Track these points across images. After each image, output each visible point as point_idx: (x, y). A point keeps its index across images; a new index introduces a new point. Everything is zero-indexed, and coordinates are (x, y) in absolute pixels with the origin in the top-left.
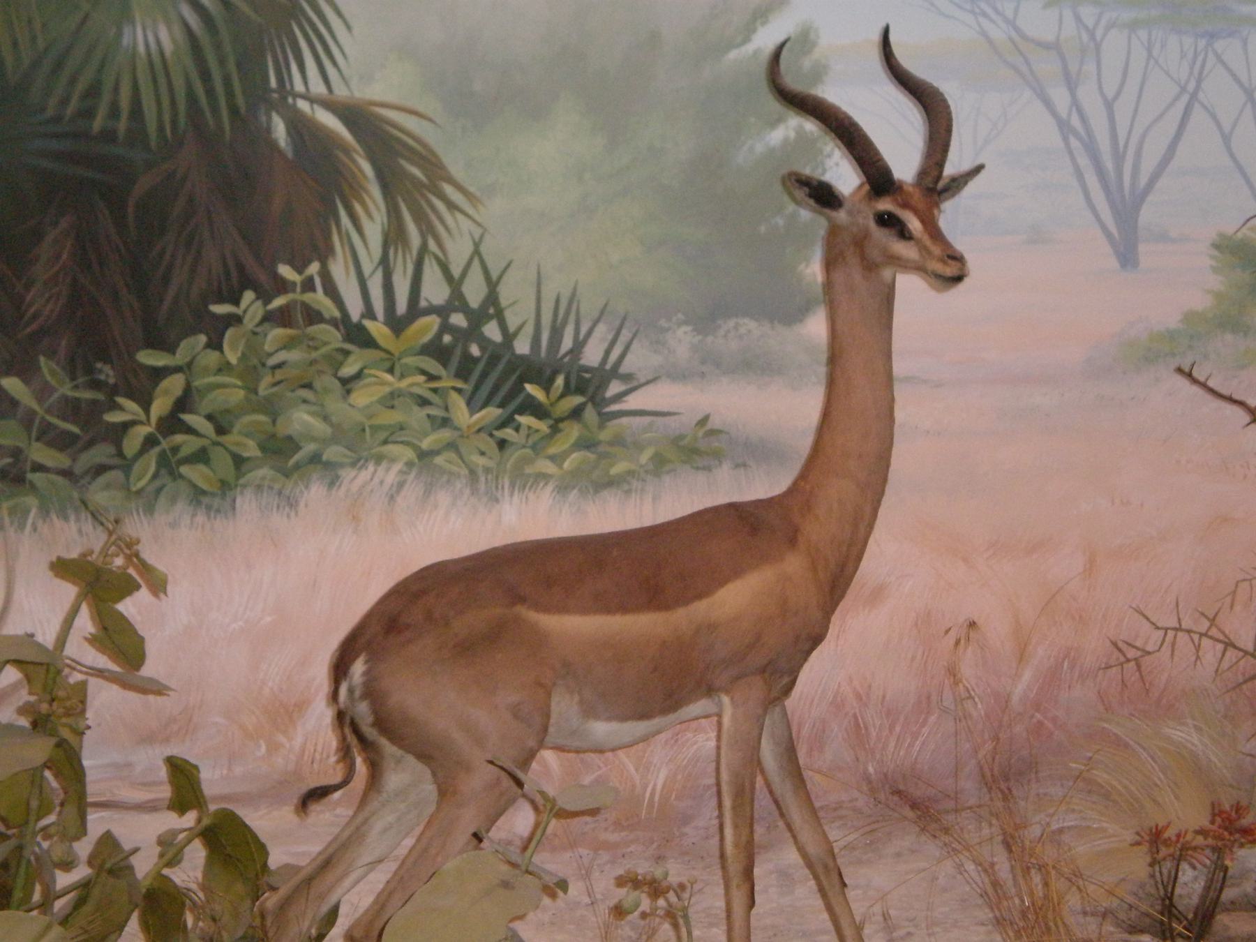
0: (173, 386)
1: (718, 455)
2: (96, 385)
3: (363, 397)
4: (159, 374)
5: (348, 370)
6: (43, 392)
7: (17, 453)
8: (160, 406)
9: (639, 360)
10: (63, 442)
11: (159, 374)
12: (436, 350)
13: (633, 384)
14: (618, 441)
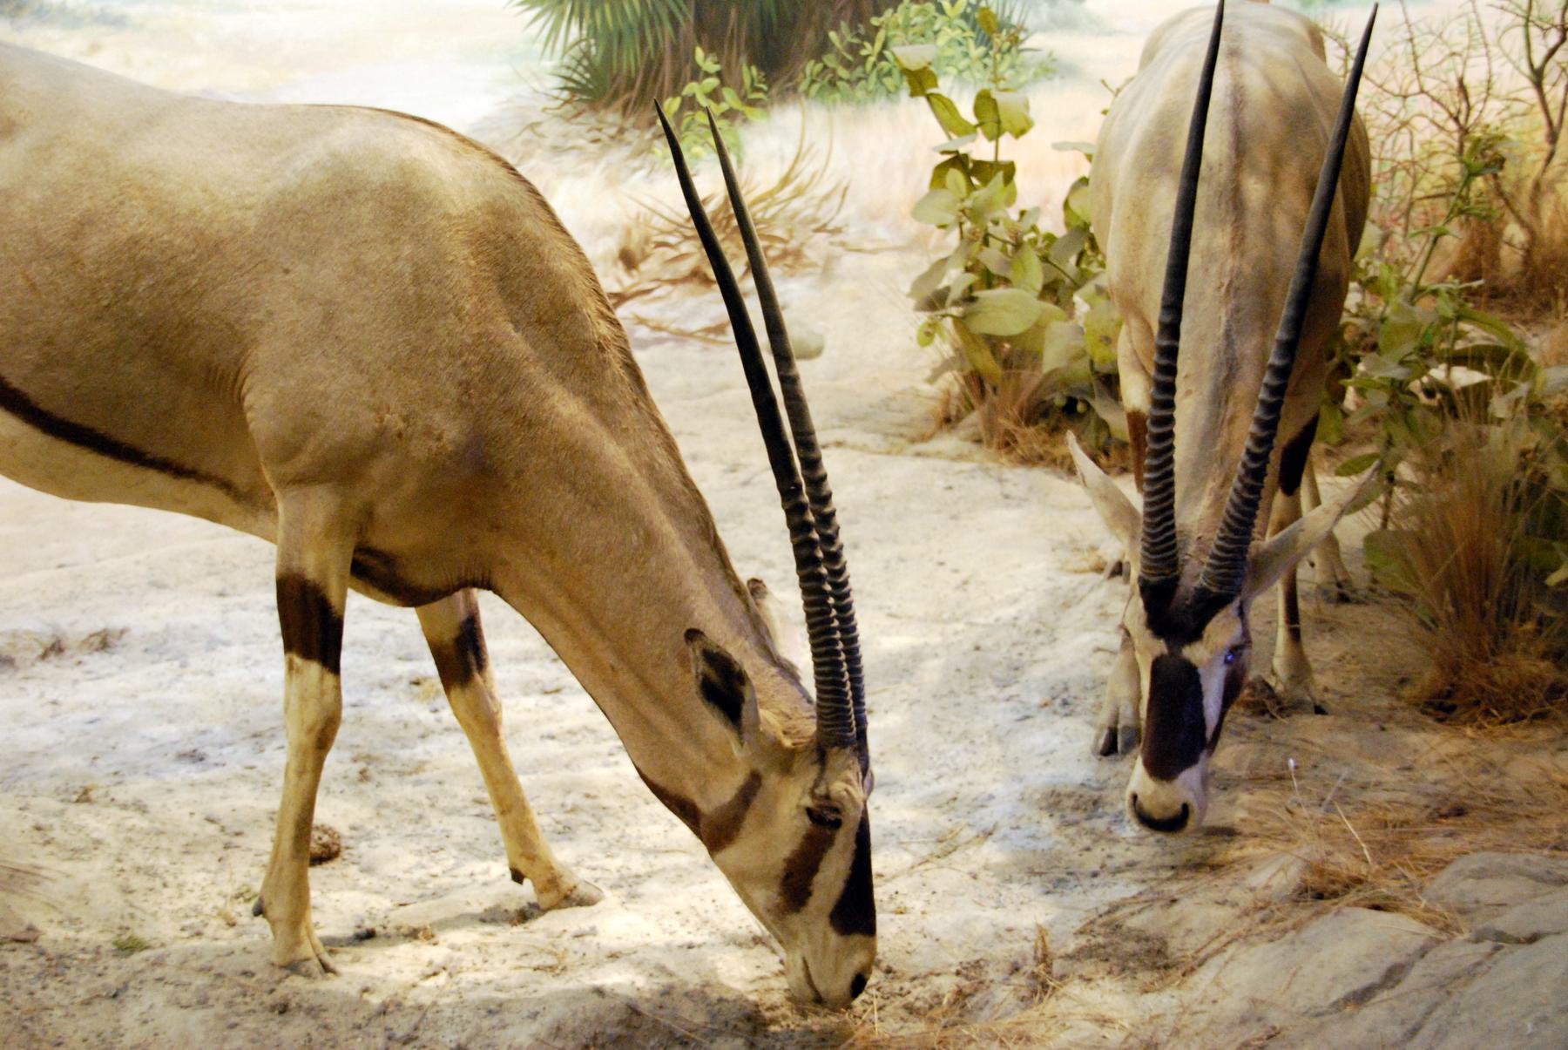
0: (881, 36)
1: (1054, 72)
2: (858, 35)
3: (942, 41)
4: (877, 29)
5: (936, 27)
6: (842, 39)
7: (834, 71)
8: (878, 45)
9: (1030, 23)
10: (849, 66)
11: (877, 29)
12: (965, 16)
13: (1029, 33)
14: (1023, 65)
